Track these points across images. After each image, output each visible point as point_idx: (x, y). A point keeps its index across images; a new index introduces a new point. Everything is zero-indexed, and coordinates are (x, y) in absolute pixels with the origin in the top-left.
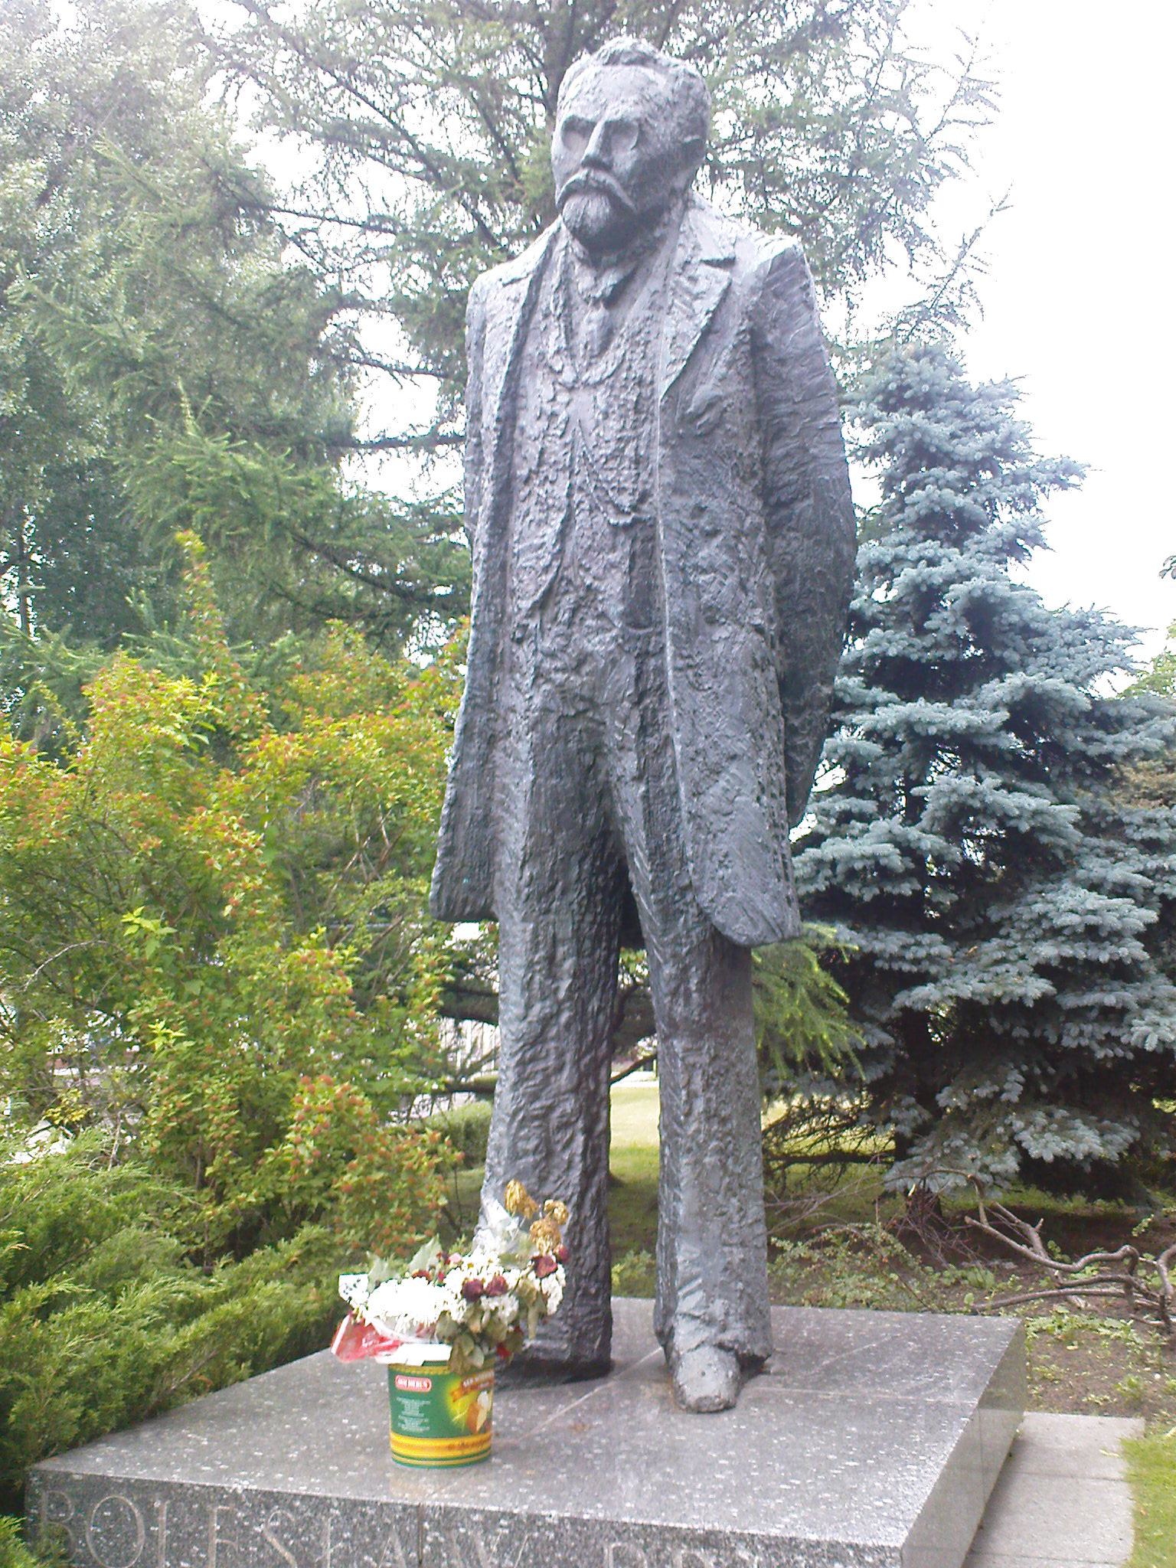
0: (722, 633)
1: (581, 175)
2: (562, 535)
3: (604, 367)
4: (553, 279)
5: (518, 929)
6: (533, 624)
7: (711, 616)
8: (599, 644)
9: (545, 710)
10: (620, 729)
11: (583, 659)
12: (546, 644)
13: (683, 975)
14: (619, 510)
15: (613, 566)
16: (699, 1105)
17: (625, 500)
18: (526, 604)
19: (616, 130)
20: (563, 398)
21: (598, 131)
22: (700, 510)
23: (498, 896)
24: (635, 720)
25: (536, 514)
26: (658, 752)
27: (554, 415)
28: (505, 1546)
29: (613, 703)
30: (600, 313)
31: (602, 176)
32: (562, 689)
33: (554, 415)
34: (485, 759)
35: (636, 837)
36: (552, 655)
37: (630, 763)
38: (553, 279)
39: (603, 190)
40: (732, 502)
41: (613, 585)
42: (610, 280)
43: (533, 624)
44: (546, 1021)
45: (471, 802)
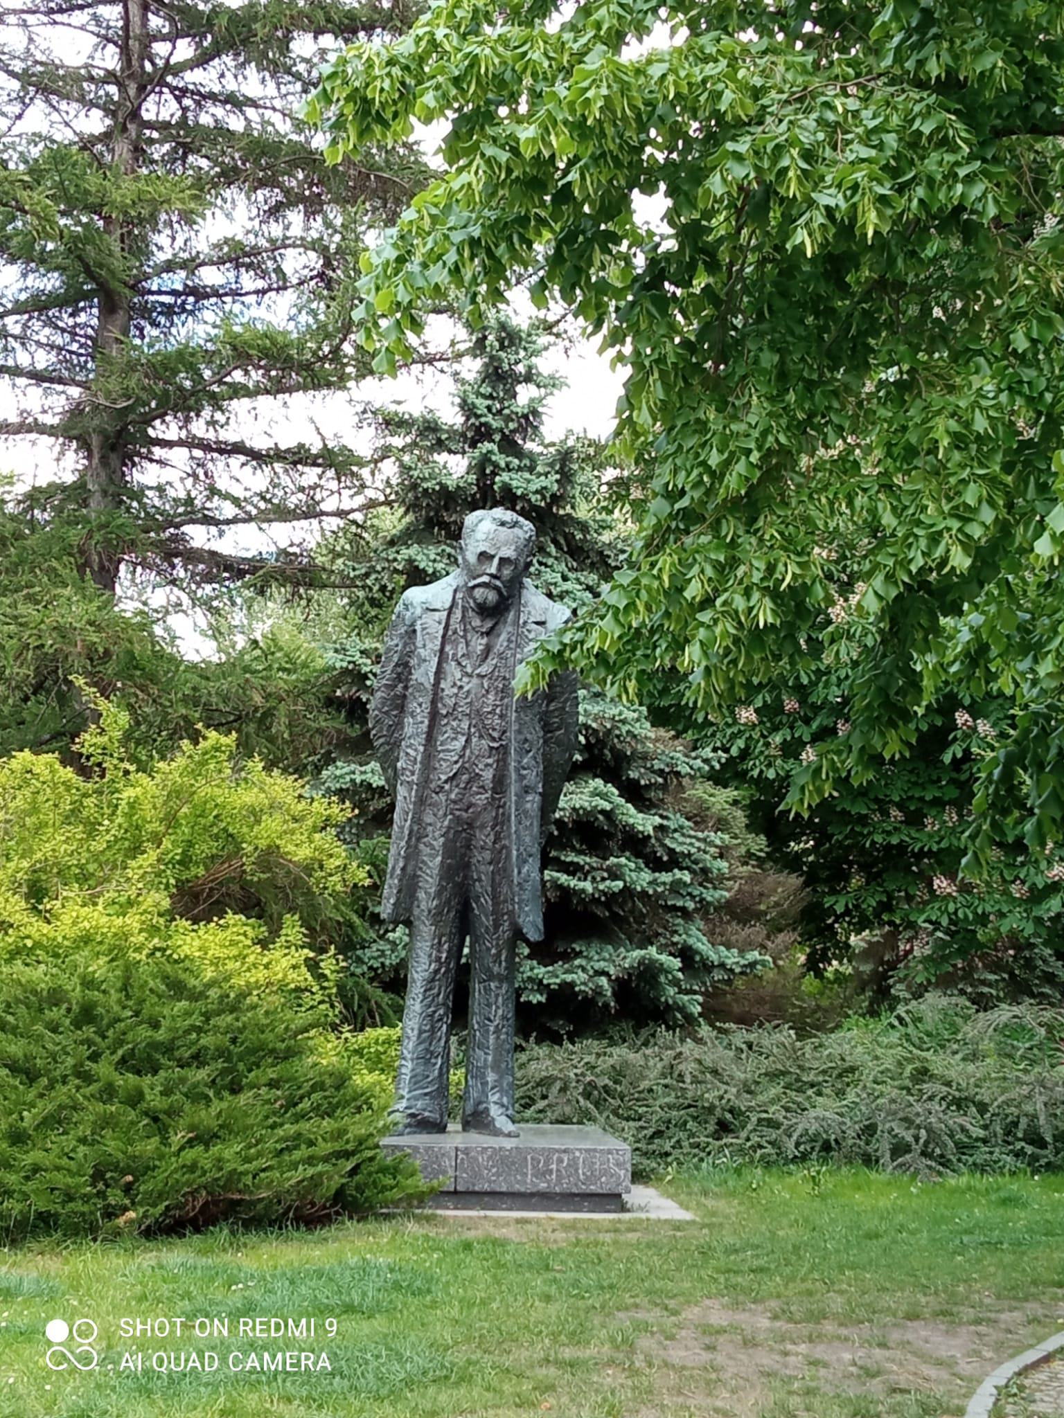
0: (529, 798)
1: (485, 579)
2: (464, 748)
3: (484, 669)
4: (458, 614)
5: (426, 930)
6: (447, 787)
7: (527, 790)
8: (481, 799)
9: (449, 828)
10: (484, 837)
11: (470, 805)
12: (453, 796)
13: (499, 954)
14: (494, 739)
15: (487, 765)
16: (500, 1012)
17: (496, 734)
18: (443, 777)
19: (503, 561)
20: (465, 679)
21: (496, 561)
22: (526, 740)
23: (416, 912)
24: (492, 837)
25: (450, 733)
26: (500, 852)
27: (461, 687)
28: (490, 1158)
29: (483, 827)
30: (485, 641)
31: (498, 583)
32: (458, 819)
33: (461, 687)
34: (416, 847)
35: (482, 887)
36: (455, 802)
37: (487, 855)
38: (458, 614)
39: (496, 588)
40: (535, 734)
41: (488, 775)
42: (489, 624)
43: (447, 787)
44: (436, 972)
45: (409, 869)
